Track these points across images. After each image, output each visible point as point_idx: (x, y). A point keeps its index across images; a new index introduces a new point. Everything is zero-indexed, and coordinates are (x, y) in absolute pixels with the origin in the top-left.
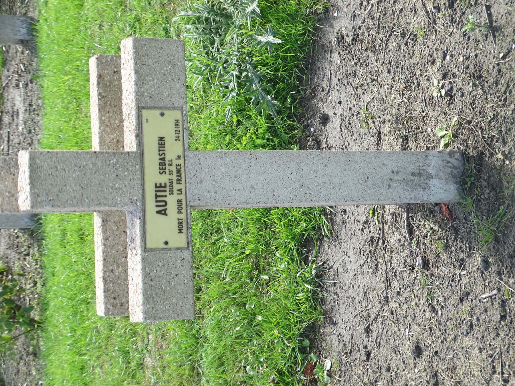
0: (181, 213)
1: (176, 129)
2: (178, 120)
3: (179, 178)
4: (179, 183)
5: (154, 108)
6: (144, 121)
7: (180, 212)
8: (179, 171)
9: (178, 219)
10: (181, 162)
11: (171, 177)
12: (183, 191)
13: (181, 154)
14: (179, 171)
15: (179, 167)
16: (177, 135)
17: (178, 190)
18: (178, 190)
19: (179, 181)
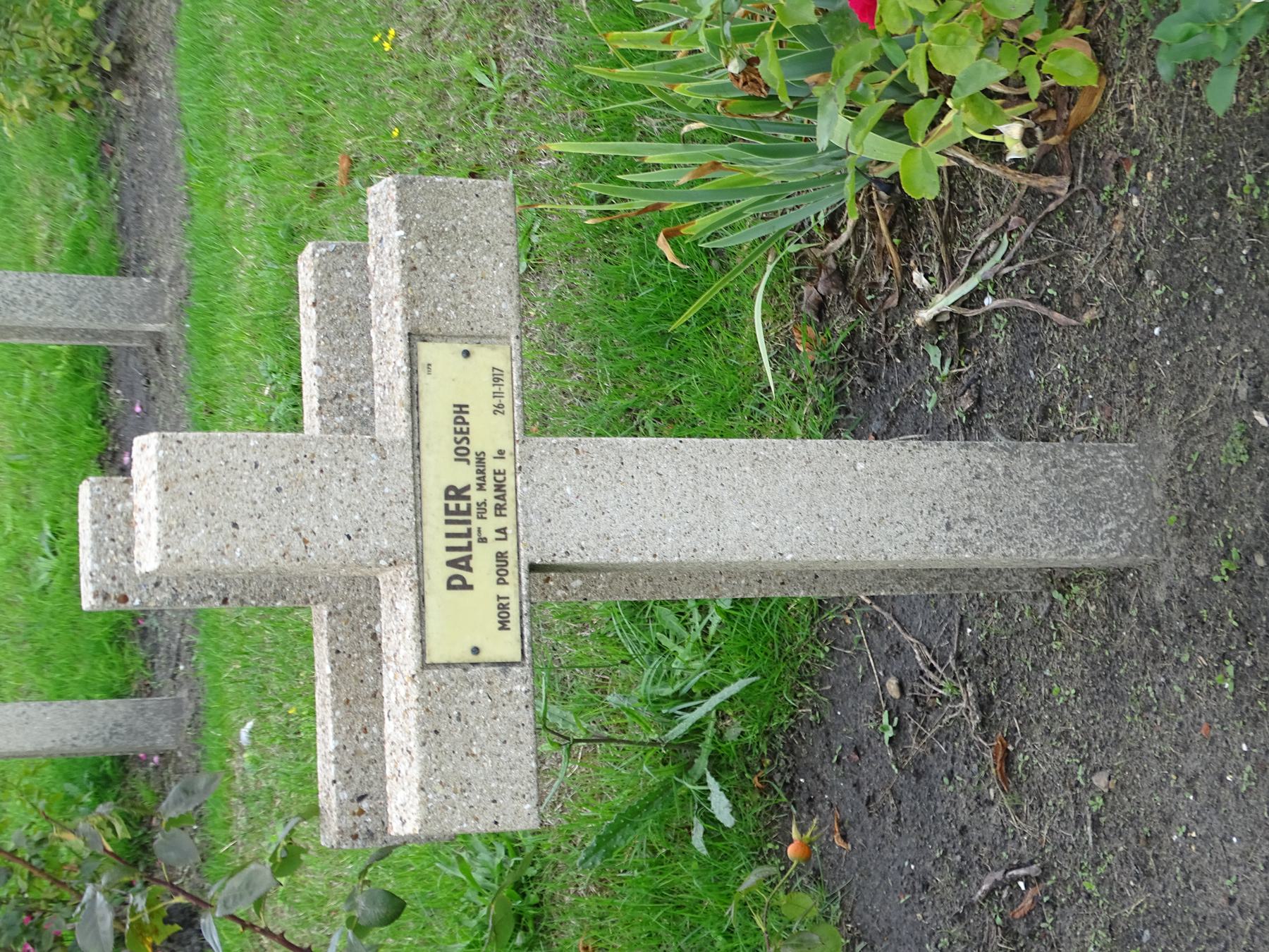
0: (505, 583)
1: (496, 389)
3: (501, 502)
4: (501, 515)
5: (446, 337)
7: (501, 581)
8: (499, 487)
9: (499, 598)
12: (509, 531)
13: (507, 446)
14: (499, 487)
15: (500, 478)
16: (496, 401)
17: (498, 531)
18: (498, 531)
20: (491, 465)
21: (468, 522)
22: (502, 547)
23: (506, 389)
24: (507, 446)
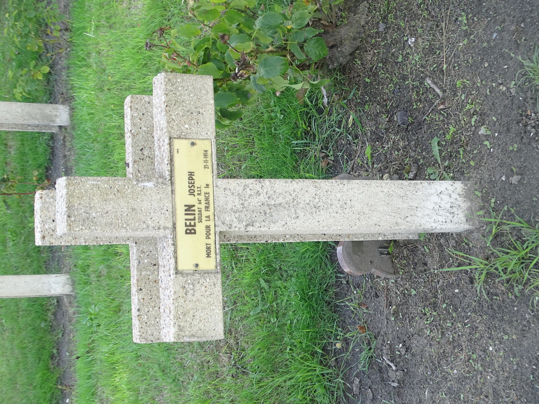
1: (205, 159)
2: (206, 151)
4: (207, 210)
6: (175, 152)
7: (208, 237)
8: (207, 199)
9: (207, 244)
10: (210, 190)
11: (200, 206)
12: (212, 217)
13: (210, 182)
14: (207, 199)
16: (205, 164)
17: (206, 217)
18: (206, 217)
19: (207, 208)
20: (204, 190)
21: (194, 214)
22: (208, 223)
23: (209, 159)
24: (210, 182)
